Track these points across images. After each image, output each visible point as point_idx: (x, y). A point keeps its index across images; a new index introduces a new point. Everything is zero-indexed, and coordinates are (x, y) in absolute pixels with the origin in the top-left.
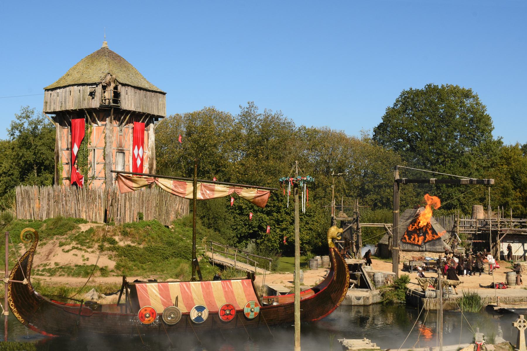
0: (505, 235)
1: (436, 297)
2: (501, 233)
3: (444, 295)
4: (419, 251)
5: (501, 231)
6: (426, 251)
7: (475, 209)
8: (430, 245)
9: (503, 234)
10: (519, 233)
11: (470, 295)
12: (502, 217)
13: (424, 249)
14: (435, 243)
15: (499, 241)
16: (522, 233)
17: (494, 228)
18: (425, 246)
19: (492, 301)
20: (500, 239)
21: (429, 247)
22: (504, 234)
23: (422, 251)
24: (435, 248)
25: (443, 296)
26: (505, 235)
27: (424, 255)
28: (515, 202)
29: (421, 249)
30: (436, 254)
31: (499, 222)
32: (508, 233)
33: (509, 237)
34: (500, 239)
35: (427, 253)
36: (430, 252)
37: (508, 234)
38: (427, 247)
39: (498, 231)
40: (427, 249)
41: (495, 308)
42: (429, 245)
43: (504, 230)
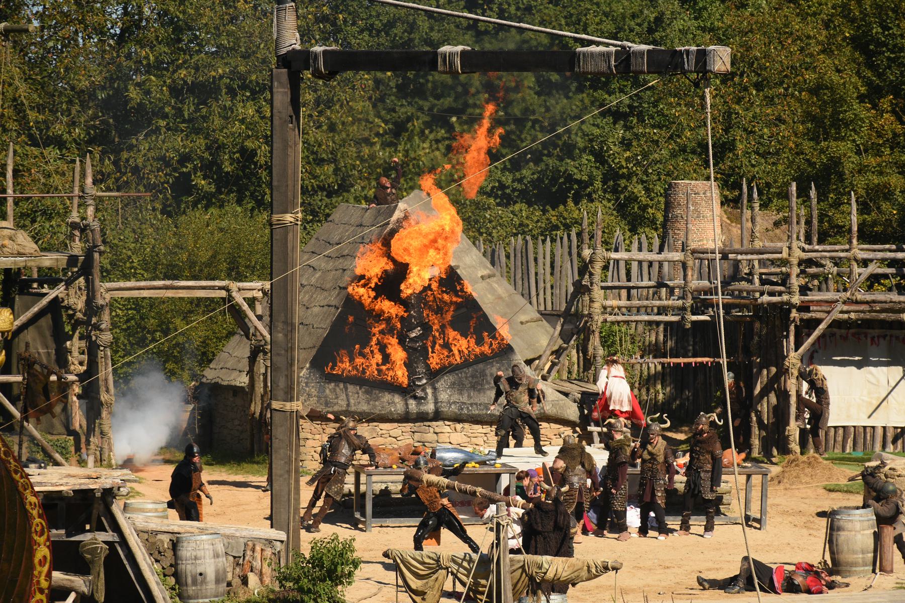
0: (822, 326)
2: (806, 316)
4: (405, 418)
5: (804, 308)
6: (438, 416)
7: (681, 198)
8: (458, 387)
9: (813, 324)
10: (892, 317)
12: (808, 240)
13: (430, 407)
17: (771, 294)
18: (435, 389)
21: (456, 397)
22: (819, 321)
23: (422, 418)
26: (822, 326)
27: (430, 437)
28: (872, 161)
29: (412, 404)
31: (795, 261)
32: (836, 315)
33: (845, 338)
35: (439, 425)
36: (458, 419)
37: (836, 324)
38: (443, 396)
39: (793, 306)
40: (444, 409)
42: (452, 386)
43: (819, 302)
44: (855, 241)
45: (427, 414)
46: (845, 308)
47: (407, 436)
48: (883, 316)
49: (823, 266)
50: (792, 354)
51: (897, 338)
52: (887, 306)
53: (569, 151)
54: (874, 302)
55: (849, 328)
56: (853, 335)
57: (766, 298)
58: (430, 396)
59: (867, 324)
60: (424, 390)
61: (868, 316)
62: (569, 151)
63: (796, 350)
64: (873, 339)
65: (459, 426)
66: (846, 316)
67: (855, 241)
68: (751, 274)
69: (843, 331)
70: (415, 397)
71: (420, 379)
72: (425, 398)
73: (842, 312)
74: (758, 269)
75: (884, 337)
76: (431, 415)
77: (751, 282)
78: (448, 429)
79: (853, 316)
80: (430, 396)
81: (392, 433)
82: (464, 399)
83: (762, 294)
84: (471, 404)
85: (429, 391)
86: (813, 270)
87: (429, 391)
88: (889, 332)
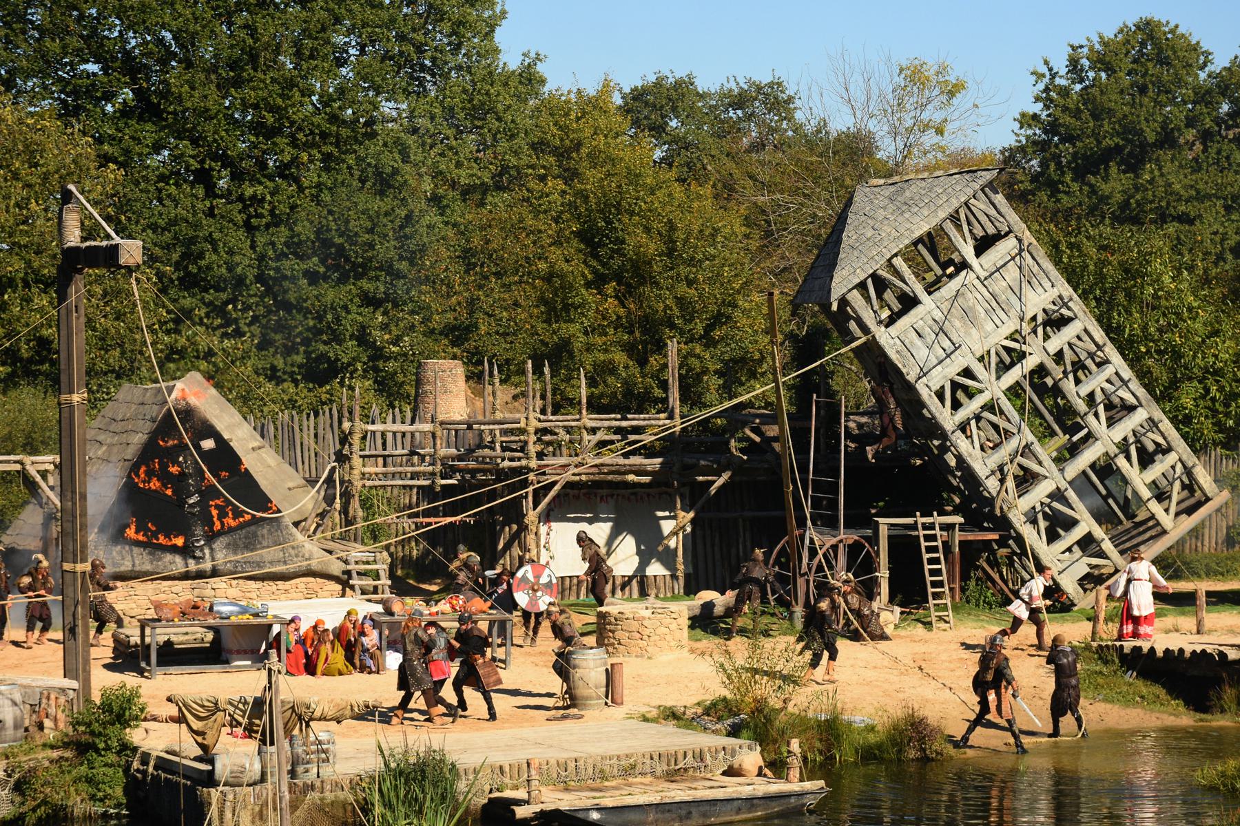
0: (557, 488)
1: (263, 779)
3: (300, 769)
4: (186, 576)
6: (215, 573)
7: (430, 375)
8: (234, 547)
10: (618, 478)
11: (412, 760)
13: (207, 566)
14: (255, 535)
15: (531, 516)
16: (631, 477)
17: (511, 459)
18: (212, 549)
19: (507, 780)
20: (536, 505)
22: (554, 483)
23: (200, 575)
25: (293, 773)
26: (557, 488)
27: (209, 592)
28: (599, 340)
30: (259, 584)
31: (531, 430)
32: (568, 476)
33: (577, 497)
34: (536, 505)
37: (569, 485)
41: (521, 812)
42: (228, 546)
44: (584, 412)
45: (205, 572)
46: (577, 471)
47: (188, 592)
48: (610, 477)
49: (556, 434)
50: (531, 512)
51: (623, 497)
52: (613, 468)
54: (602, 465)
55: (580, 489)
56: (584, 494)
57: (506, 464)
58: (207, 556)
59: (597, 485)
60: (202, 550)
61: (597, 478)
63: (534, 509)
64: (602, 498)
65: (234, 582)
66: (577, 478)
67: (584, 412)
68: (493, 442)
69: (576, 492)
70: (194, 557)
71: (198, 541)
72: (203, 558)
73: (574, 475)
74: (499, 438)
75: (612, 496)
76: (209, 573)
77: (493, 449)
78: (224, 585)
79: (584, 478)
80: (207, 556)
81: (174, 590)
82: (239, 557)
83: (503, 459)
84: (245, 563)
85: (207, 551)
86: (548, 438)
87: (207, 551)
88: (616, 492)
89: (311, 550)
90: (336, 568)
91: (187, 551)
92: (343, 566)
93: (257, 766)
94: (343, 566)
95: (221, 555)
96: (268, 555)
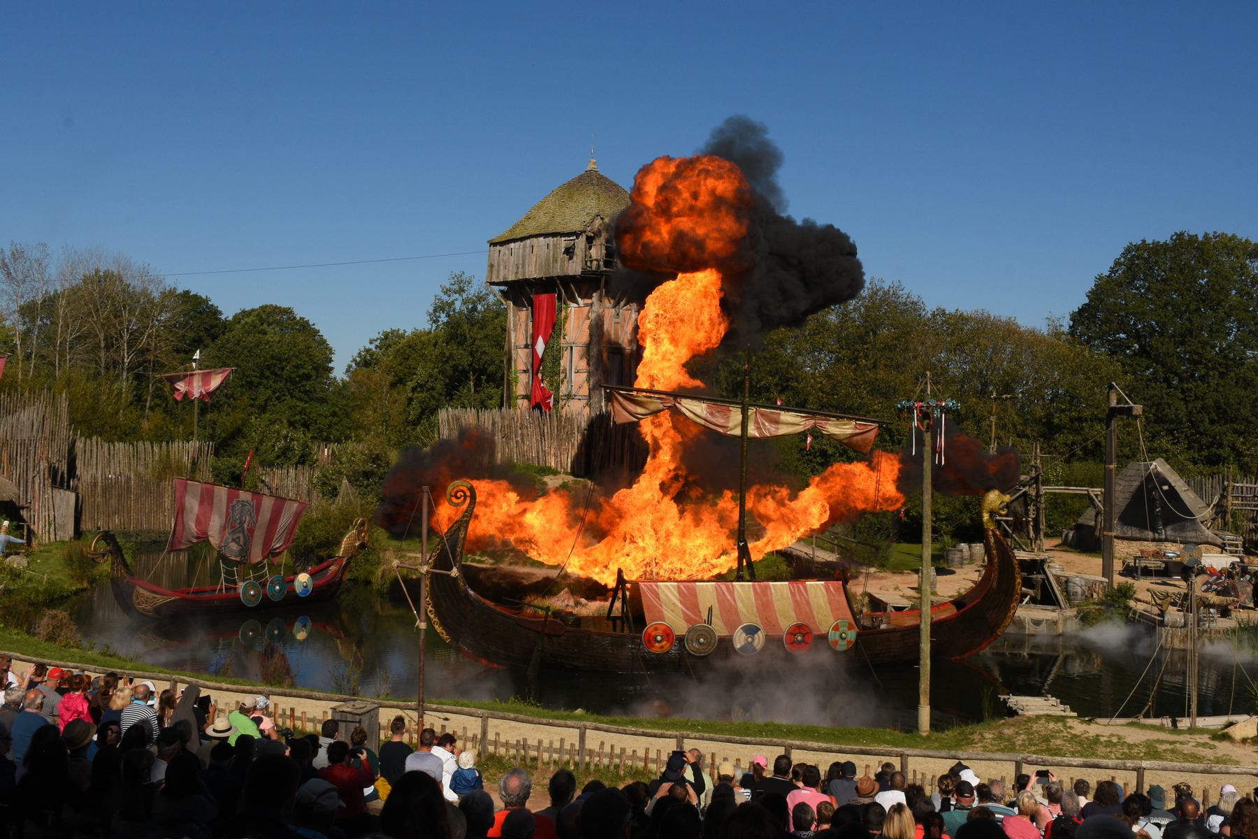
1: (1185, 625)
3: (1201, 623)
4: (1154, 540)
6: (1166, 540)
8: (1174, 530)
13: (1164, 537)
23: (1160, 540)
24: (1184, 535)
25: (1198, 626)
27: (1164, 548)
29: (1156, 535)
35: (1169, 545)
38: (1169, 533)
40: (1169, 538)
42: (1172, 529)
53: (1221, 446)
62: (1221, 446)
89: (1209, 533)
90: (1219, 541)
91: (1154, 530)
92: (1222, 541)
93: (1183, 620)
94: (1222, 541)
95: (1169, 532)
96: (1190, 535)
